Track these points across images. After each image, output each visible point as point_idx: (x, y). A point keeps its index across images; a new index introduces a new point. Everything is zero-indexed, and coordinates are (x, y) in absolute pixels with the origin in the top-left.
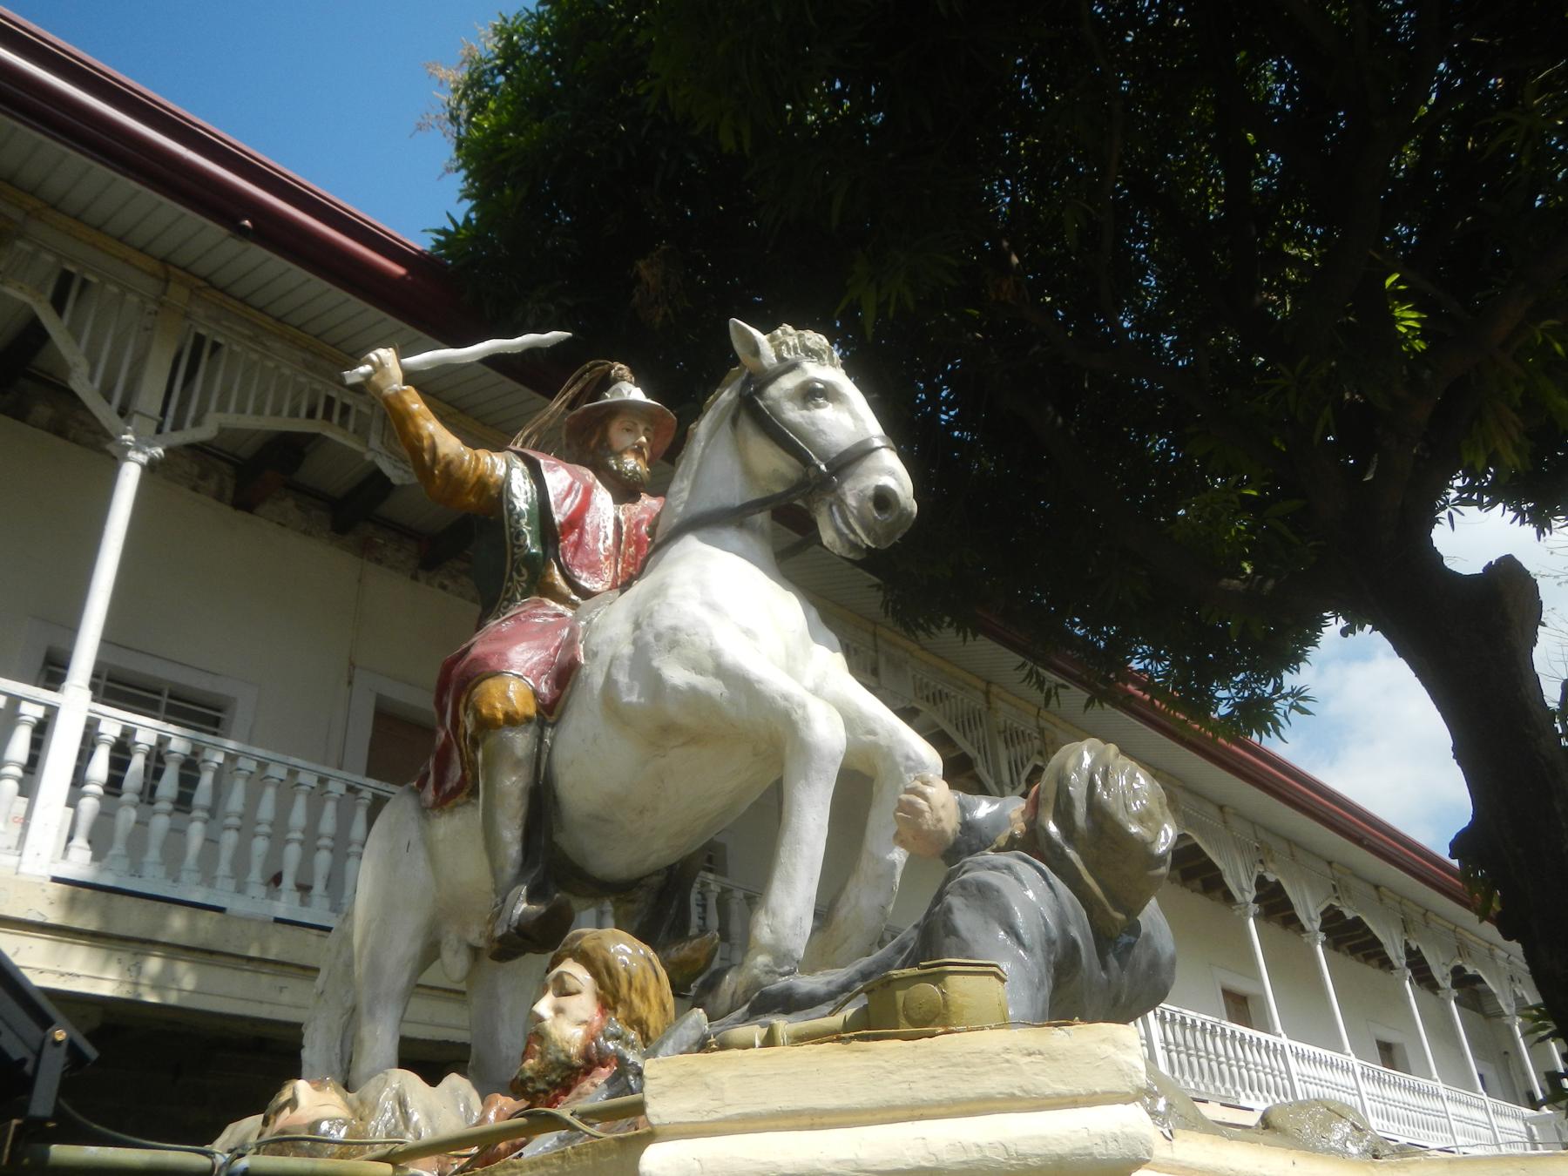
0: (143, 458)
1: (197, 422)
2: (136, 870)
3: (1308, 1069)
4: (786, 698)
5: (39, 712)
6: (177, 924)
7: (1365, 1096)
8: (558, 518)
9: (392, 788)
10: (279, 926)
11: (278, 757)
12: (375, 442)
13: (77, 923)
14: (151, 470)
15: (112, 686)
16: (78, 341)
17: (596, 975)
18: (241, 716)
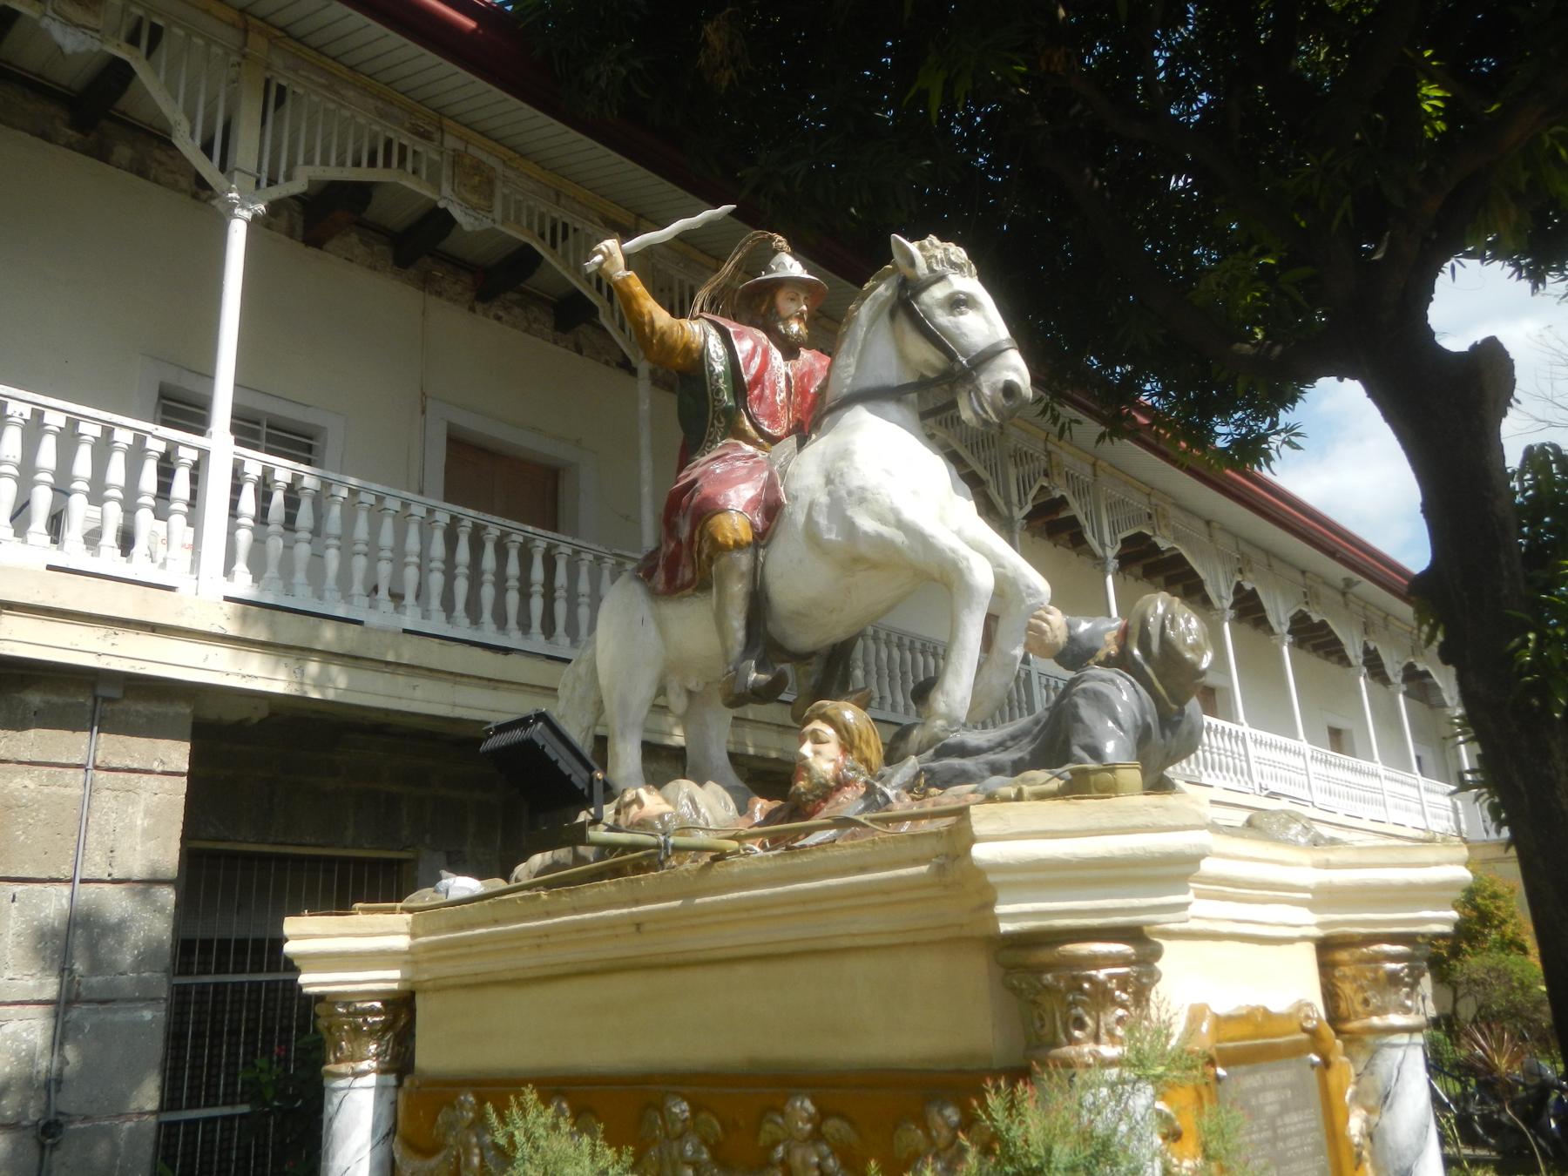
0: (248, 215)
1: (289, 178)
2: (289, 590)
3: (1265, 753)
4: (953, 551)
5: (194, 455)
6: (328, 635)
7: (1312, 776)
8: (746, 378)
9: (488, 517)
10: (408, 636)
11: (393, 491)
12: (446, 189)
13: (251, 635)
14: (254, 224)
15: (247, 429)
16: (176, 98)
17: (838, 731)
18: (333, 445)
